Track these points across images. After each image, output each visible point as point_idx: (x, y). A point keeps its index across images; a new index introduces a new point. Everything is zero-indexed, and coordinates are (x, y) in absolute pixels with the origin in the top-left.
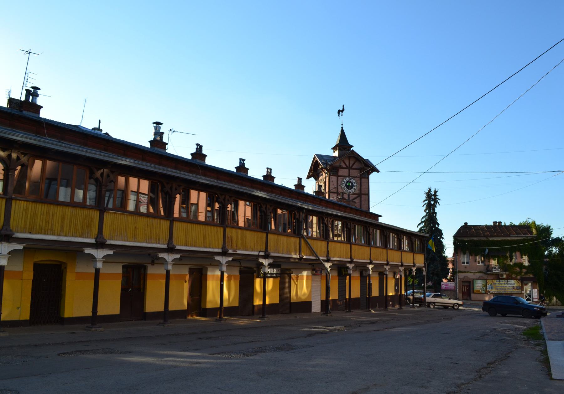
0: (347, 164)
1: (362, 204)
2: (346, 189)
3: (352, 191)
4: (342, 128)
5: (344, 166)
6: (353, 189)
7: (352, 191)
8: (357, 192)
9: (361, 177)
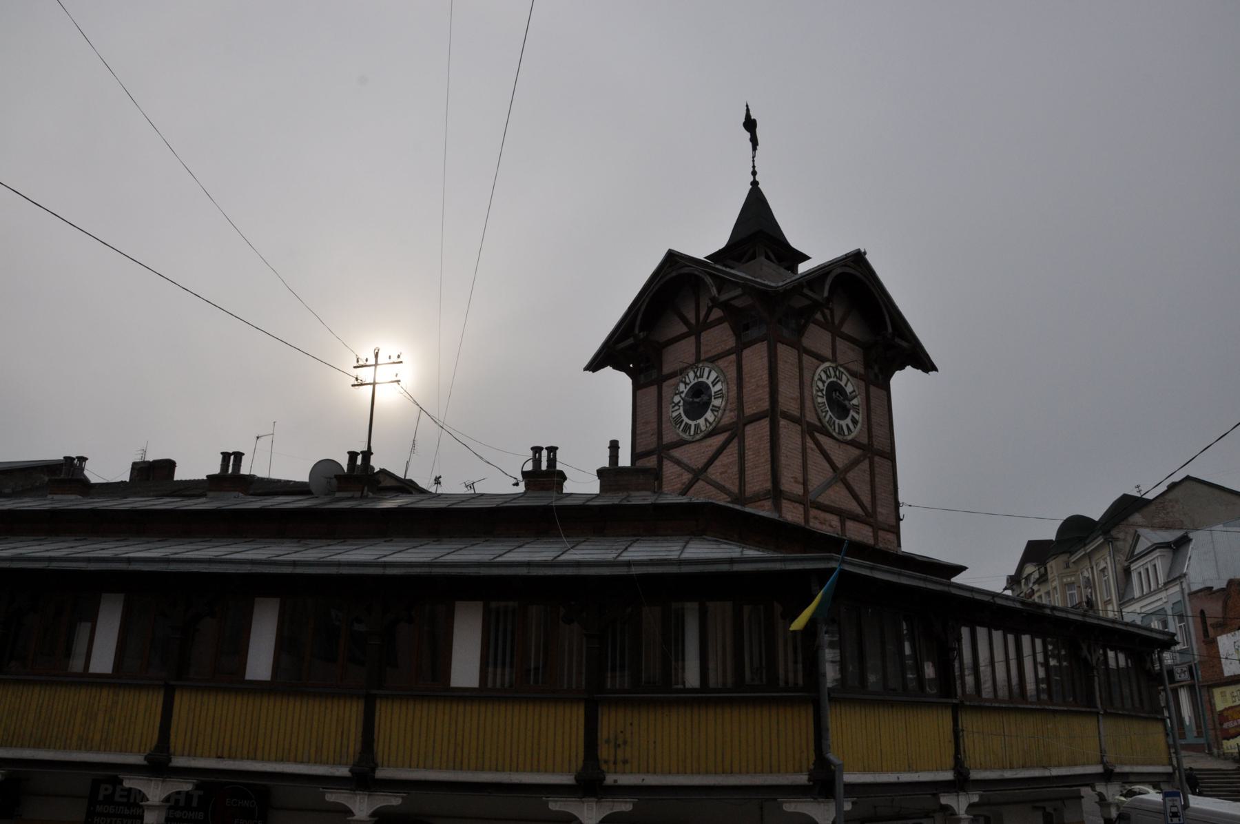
0: (691, 316)
1: (748, 465)
2: (686, 420)
3: (706, 420)
4: (755, 184)
5: (684, 329)
6: (709, 411)
7: (706, 420)
8: (728, 418)
9: (738, 351)
